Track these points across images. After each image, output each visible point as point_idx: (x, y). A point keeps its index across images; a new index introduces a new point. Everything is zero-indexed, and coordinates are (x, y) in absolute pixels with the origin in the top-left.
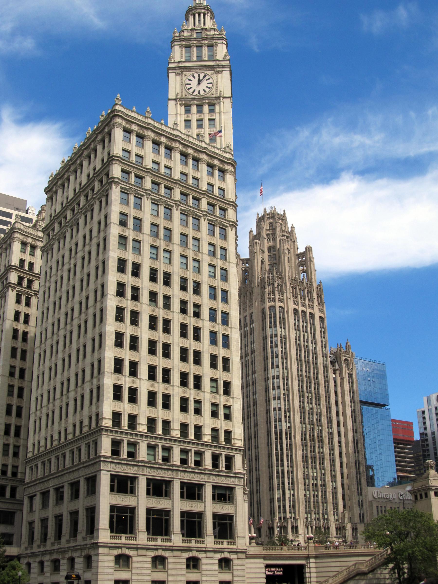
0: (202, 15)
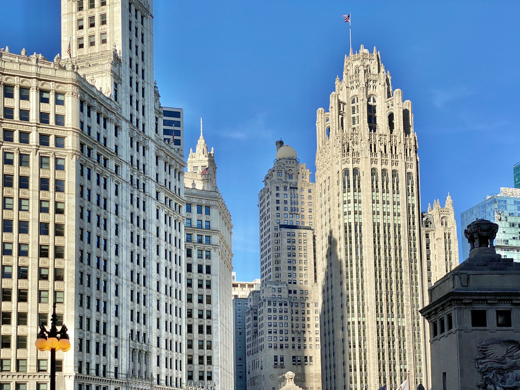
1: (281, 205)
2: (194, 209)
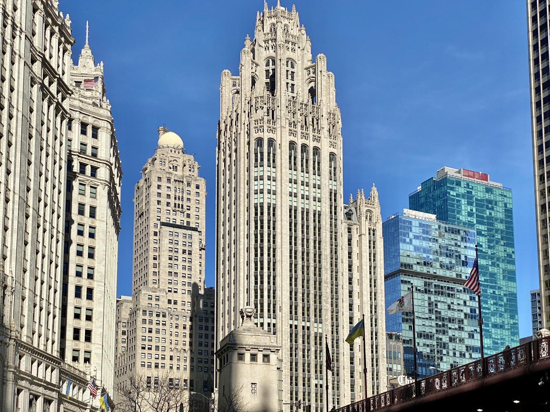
1: (164, 200)
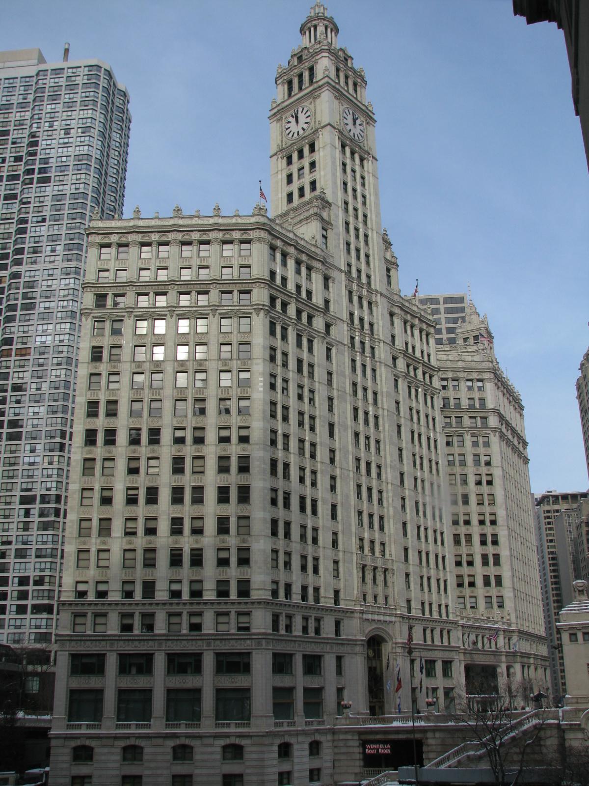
0: (312, 29)
2: (464, 385)
